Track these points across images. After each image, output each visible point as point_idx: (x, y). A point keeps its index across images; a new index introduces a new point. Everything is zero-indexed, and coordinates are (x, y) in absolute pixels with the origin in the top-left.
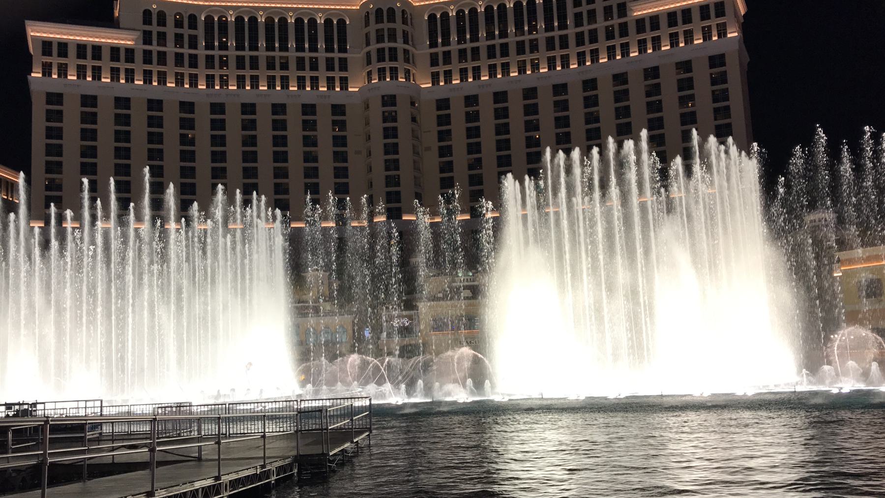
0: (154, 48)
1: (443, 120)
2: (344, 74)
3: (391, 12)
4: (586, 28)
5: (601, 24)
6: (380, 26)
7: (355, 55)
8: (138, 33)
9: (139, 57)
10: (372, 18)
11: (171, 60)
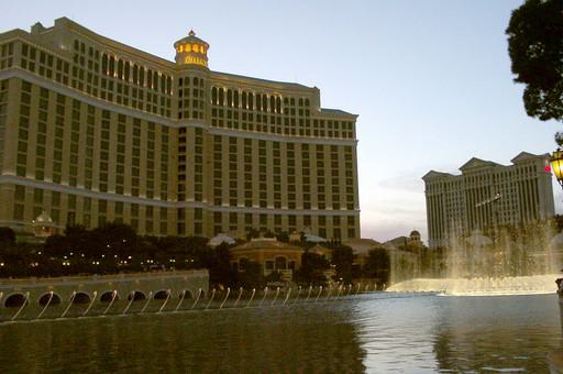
0: (79, 65)
5: (297, 116)
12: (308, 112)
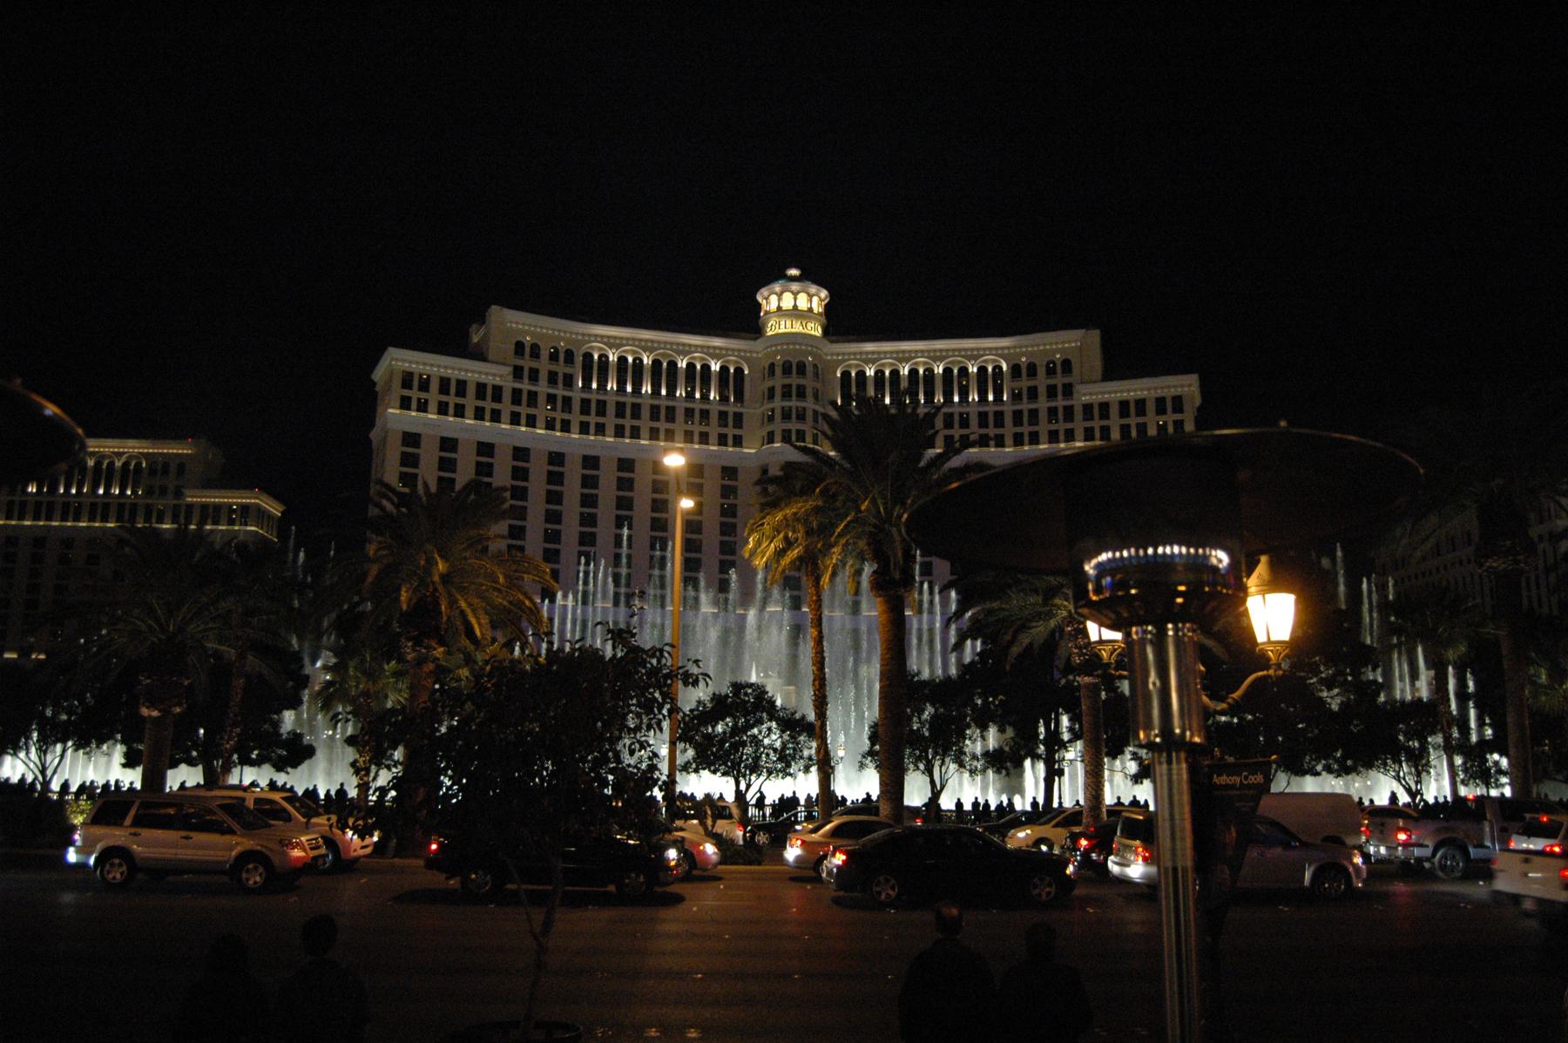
0: (525, 386)
2: (738, 432)
3: (801, 369)
4: (1025, 406)
5: (1043, 404)
6: (787, 381)
7: (753, 410)
8: (510, 369)
9: (507, 396)
10: (778, 370)
12: (1068, 390)
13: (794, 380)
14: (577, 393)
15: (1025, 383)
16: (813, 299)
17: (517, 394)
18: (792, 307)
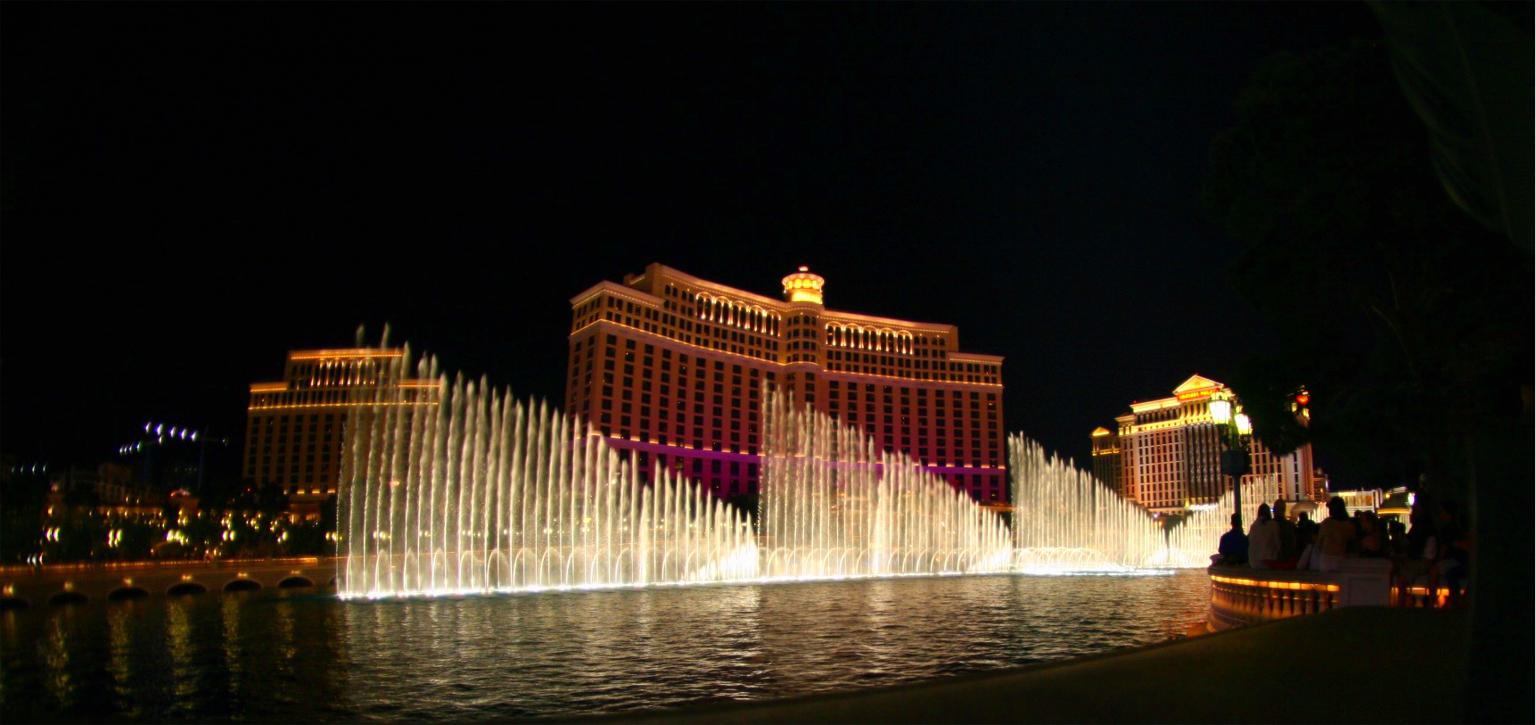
1: (834, 395)
4: (921, 359)
6: (807, 327)
9: (661, 317)
10: (802, 320)
11: (677, 322)
12: (943, 354)
13: (810, 327)
14: (694, 321)
15: (921, 347)
16: (817, 283)
17: (665, 316)
18: (805, 288)
